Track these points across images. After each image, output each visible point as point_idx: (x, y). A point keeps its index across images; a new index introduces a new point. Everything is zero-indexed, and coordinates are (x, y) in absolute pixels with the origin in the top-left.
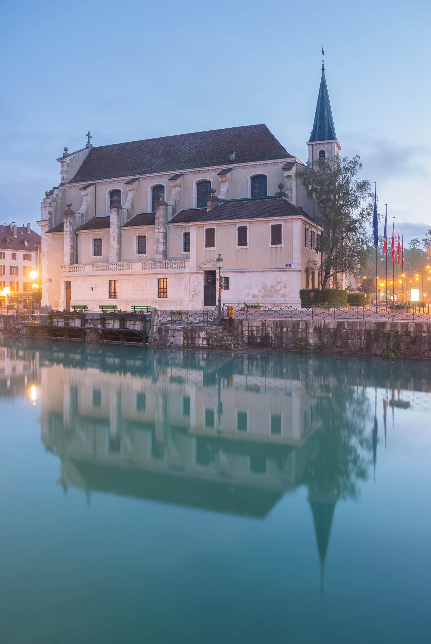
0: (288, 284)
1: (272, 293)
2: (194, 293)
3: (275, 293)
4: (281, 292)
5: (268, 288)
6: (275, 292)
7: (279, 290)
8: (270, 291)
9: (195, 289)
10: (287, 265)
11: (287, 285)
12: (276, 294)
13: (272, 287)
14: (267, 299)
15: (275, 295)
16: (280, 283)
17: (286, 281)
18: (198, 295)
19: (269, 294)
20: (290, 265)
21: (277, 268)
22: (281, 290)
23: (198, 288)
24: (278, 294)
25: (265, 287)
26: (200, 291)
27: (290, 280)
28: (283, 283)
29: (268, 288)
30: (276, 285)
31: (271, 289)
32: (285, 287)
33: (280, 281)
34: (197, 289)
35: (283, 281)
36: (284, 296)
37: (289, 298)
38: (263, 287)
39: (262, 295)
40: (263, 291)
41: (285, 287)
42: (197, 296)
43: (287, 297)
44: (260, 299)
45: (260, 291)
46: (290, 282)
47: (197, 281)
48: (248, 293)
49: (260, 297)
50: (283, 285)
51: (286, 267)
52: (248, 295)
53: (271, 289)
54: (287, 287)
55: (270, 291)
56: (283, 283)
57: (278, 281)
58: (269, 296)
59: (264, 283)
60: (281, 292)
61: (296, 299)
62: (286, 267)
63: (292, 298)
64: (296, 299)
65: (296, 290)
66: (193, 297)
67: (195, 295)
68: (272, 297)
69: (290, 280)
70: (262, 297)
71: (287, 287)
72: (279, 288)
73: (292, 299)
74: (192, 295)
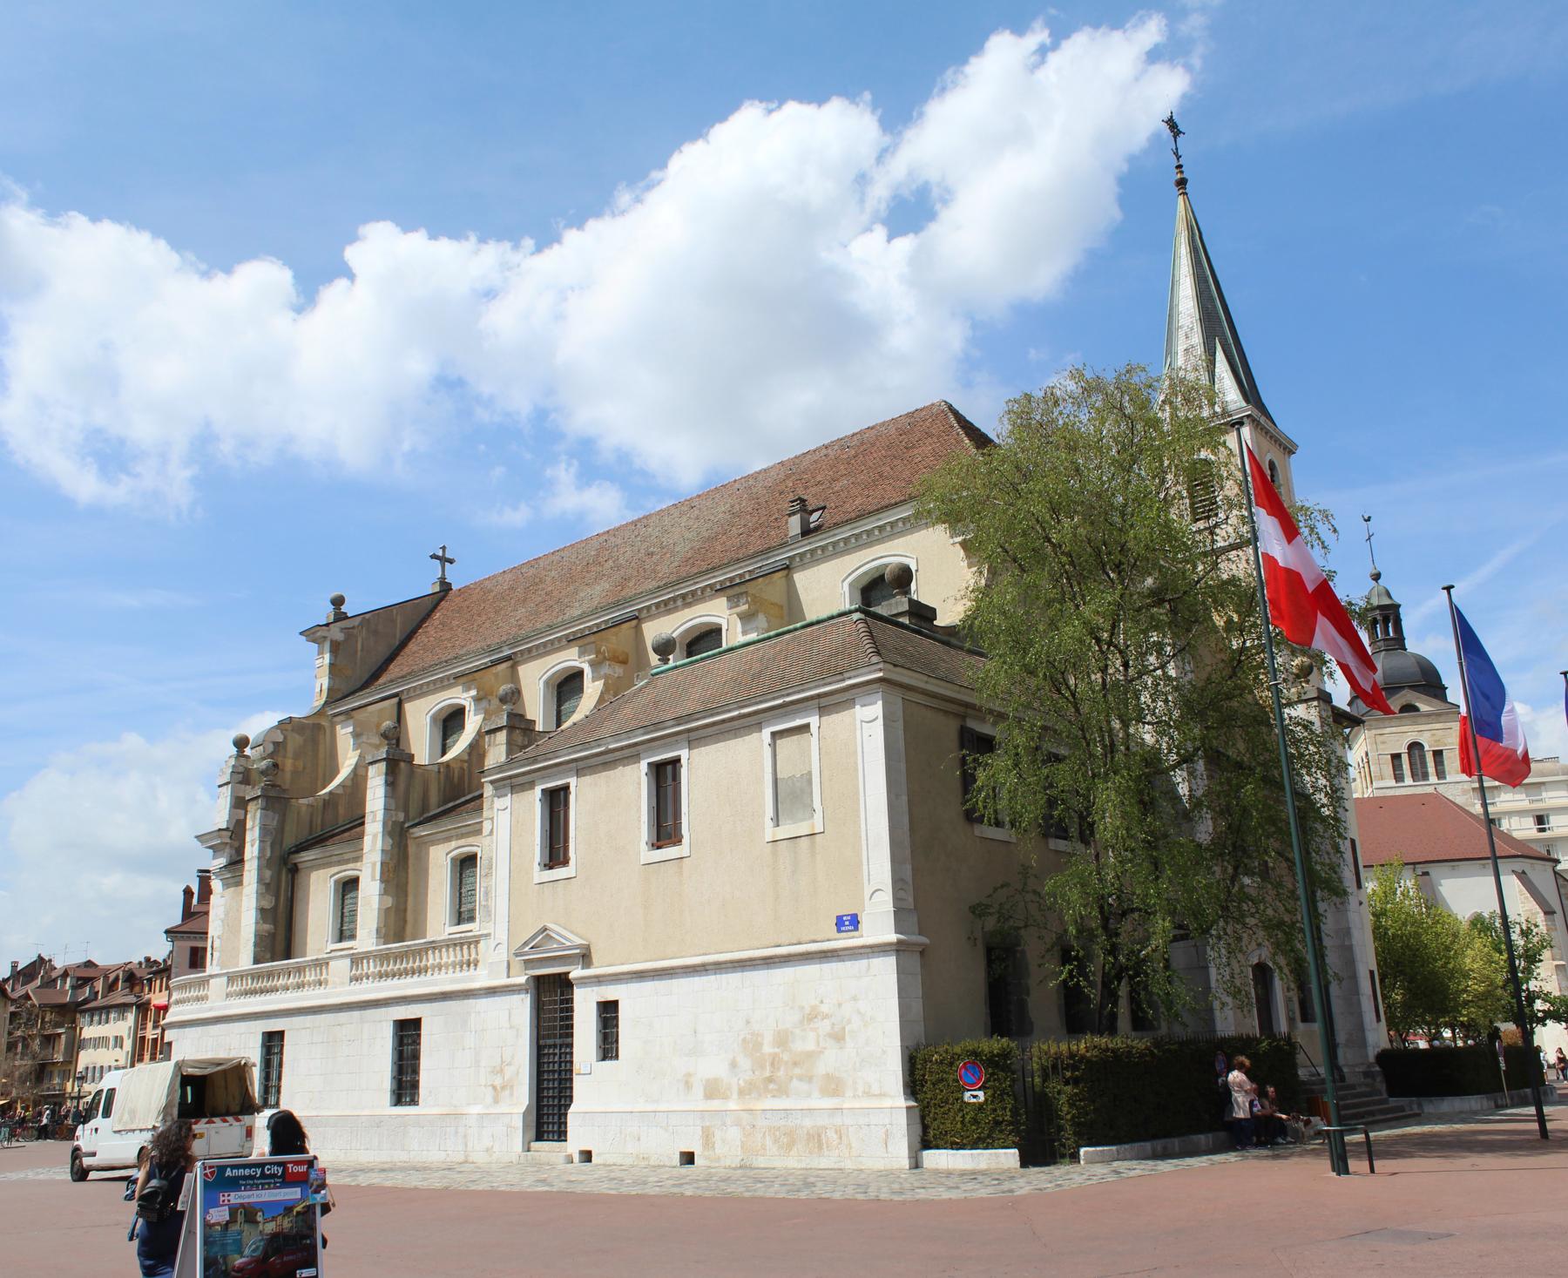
0: (849, 1022)
1: (781, 1073)
2: (498, 1082)
3: (797, 1071)
4: (822, 1067)
5: (768, 1049)
6: (795, 1064)
7: (810, 1056)
8: (772, 1064)
9: (502, 1062)
10: (840, 922)
11: (844, 1028)
12: (800, 1079)
13: (782, 1039)
14: (760, 1105)
15: (795, 1083)
16: (812, 1016)
17: (840, 1005)
18: (512, 1087)
19: (770, 1080)
20: (855, 921)
21: (800, 943)
22: (821, 1052)
23: (513, 1057)
24: (810, 1079)
25: (752, 1044)
26: (518, 1073)
27: (855, 999)
28: (826, 1016)
29: (768, 1049)
30: (797, 1031)
31: (777, 1050)
32: (838, 1037)
33: (814, 1008)
34: (509, 1064)
35: (825, 1008)
36: (833, 1086)
37: (854, 1096)
38: (744, 1040)
39: (741, 1082)
40: (745, 1063)
41: (838, 1037)
42: (507, 1092)
43: (849, 1093)
44: (732, 1105)
45: (734, 1065)
46: (859, 1013)
47: (511, 1027)
48: (689, 1075)
49: (735, 1096)
50: (824, 1026)
51: (839, 931)
52: (688, 1085)
53: (777, 1050)
54: (847, 1038)
55: (775, 1062)
56: (826, 1016)
57: (807, 1010)
58: (771, 1086)
59: (748, 1022)
60: (822, 1067)
61: (887, 1103)
62: (839, 931)
63: (868, 1094)
64: (887, 1103)
65: (884, 1052)
66: (496, 1101)
67: (503, 1088)
68: (782, 1091)
69: (855, 999)
70: (741, 1093)
71: (844, 1039)
72: (810, 1046)
73: (866, 1103)
74: (494, 1088)
